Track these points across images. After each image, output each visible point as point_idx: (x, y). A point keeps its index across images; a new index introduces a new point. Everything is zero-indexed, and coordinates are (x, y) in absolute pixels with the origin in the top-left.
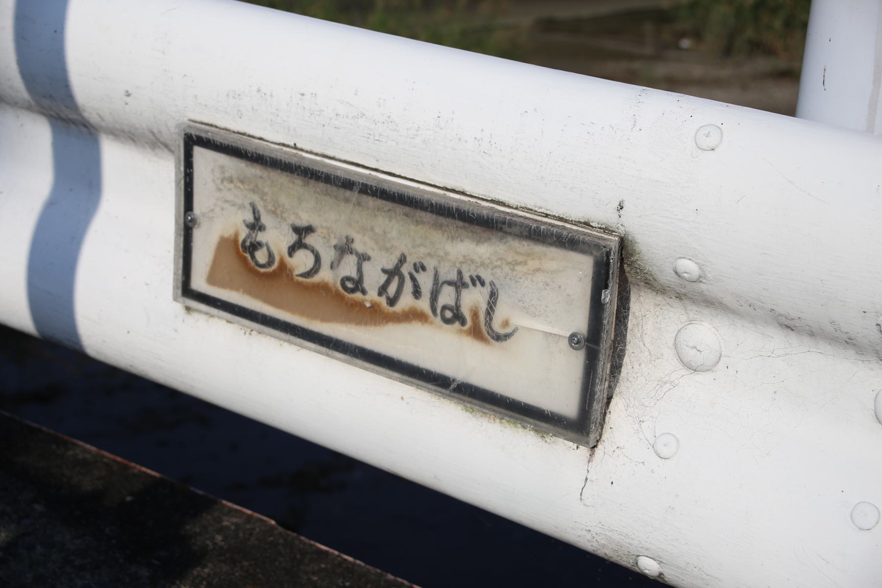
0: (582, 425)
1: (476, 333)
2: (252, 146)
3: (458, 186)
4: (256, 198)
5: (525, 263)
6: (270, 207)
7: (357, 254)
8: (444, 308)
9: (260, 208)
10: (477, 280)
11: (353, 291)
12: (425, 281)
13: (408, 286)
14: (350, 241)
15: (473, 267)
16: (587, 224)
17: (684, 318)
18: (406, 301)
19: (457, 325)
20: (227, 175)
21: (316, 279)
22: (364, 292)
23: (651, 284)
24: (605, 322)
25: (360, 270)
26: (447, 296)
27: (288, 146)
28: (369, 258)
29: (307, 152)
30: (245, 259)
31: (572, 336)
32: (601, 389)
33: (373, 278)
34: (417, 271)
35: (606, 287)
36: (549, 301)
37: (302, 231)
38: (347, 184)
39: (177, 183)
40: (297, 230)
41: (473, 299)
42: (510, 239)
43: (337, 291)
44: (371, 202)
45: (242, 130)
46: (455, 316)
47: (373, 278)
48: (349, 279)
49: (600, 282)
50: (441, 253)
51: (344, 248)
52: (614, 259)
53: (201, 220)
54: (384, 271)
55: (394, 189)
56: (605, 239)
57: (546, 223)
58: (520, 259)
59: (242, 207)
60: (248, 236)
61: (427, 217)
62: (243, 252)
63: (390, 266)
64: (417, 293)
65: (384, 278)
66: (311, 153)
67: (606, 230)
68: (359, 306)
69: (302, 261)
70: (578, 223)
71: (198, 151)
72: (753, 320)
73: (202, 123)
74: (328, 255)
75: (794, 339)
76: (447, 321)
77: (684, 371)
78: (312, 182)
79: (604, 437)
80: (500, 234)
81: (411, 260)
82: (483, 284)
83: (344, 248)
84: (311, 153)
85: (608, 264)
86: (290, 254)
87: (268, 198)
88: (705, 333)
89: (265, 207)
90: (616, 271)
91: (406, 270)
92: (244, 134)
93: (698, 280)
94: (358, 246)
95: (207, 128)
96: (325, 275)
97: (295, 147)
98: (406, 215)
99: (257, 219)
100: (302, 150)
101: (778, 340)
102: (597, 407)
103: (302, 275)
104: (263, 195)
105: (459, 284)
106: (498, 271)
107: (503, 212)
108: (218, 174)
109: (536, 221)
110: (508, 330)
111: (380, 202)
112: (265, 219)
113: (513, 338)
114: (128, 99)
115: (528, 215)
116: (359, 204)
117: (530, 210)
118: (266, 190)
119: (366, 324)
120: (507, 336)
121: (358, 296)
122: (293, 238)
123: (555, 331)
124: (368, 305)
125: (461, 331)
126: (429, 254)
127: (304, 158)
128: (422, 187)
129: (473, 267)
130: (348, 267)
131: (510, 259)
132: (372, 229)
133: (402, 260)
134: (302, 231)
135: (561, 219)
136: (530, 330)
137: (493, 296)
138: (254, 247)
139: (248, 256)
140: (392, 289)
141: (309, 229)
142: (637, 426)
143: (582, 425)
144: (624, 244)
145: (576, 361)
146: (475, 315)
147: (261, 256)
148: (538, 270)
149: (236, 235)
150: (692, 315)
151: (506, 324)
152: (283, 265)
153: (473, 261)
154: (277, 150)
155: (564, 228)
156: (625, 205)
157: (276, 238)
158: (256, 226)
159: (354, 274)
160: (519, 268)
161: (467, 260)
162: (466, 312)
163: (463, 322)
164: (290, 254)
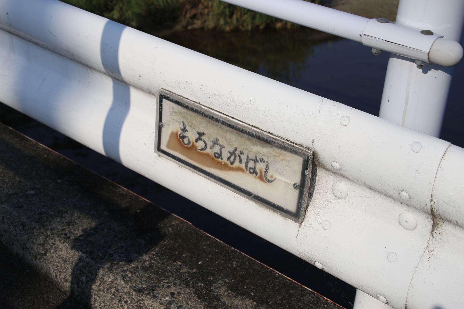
0: (297, 215)
1: (261, 178)
2: (184, 101)
3: (257, 126)
4: (184, 120)
5: (279, 157)
6: (189, 124)
7: (220, 145)
8: (250, 168)
9: (186, 123)
10: (262, 160)
11: (218, 158)
12: (244, 158)
13: (238, 159)
14: (217, 140)
15: (261, 155)
16: (301, 145)
17: (336, 180)
18: (237, 164)
19: (254, 174)
20: (175, 111)
21: (205, 152)
22: (222, 159)
23: (324, 167)
24: (306, 181)
25: (221, 151)
26: (251, 164)
27: (197, 103)
28: (224, 147)
29: (203, 106)
30: (180, 141)
31: (294, 185)
32: (304, 204)
33: (225, 154)
34: (241, 154)
35: (307, 169)
36: (287, 172)
37: (201, 134)
38: (217, 120)
39: (157, 111)
40: (199, 133)
41: (260, 166)
42: (274, 147)
43: (212, 157)
44: (225, 127)
45: (180, 94)
46: (254, 172)
47: (225, 154)
48: (217, 153)
49: (305, 167)
50: (250, 149)
51: (216, 142)
52: (310, 160)
53: (165, 125)
54: (229, 152)
55: (234, 124)
56: (307, 152)
57: (287, 144)
58: (277, 155)
59: (179, 122)
60: (181, 133)
61: (245, 136)
62: (179, 138)
63: (232, 151)
64: (241, 162)
65: (229, 155)
66: (205, 106)
67: (308, 148)
68: (220, 163)
69: (200, 145)
70: (298, 145)
71: (164, 101)
72: (359, 184)
73: (166, 90)
74: (209, 144)
75: (373, 192)
76: (251, 173)
77: (334, 198)
78: (205, 118)
79: (305, 220)
80: (271, 145)
81: (239, 150)
82: (264, 162)
83: (216, 142)
84: (205, 106)
85: (308, 161)
86: (196, 142)
87: (189, 121)
88: (343, 186)
89: (188, 124)
90: (311, 163)
91: (237, 153)
92: (181, 96)
93: (340, 169)
94: (220, 142)
95: (168, 92)
96: (208, 151)
97: (199, 103)
98: (238, 134)
99: (185, 128)
100: (202, 105)
101: (367, 192)
102: (302, 210)
103: (200, 150)
104: (187, 119)
105: (256, 161)
106: (269, 158)
107: (272, 138)
108: (171, 110)
109: (284, 142)
110: (273, 179)
111: (228, 128)
112: (187, 128)
113: (274, 182)
114: (140, 78)
115: (281, 140)
116: (221, 128)
117: (282, 138)
118: (188, 118)
119: (222, 170)
120: (272, 181)
121: (220, 159)
122: (198, 136)
123: (289, 182)
124: (223, 164)
125: (256, 177)
126: (245, 149)
127: (202, 108)
128: (244, 124)
129: (261, 155)
130: (217, 149)
131: (274, 154)
132: (225, 137)
133: (236, 149)
134: (201, 134)
135: (292, 142)
136: (279, 180)
137: (268, 166)
138: (184, 137)
139: (181, 140)
140: (232, 159)
141: (203, 134)
142: (316, 217)
143: (297, 215)
144: (314, 154)
145: (296, 193)
146: (261, 172)
147: (186, 141)
148: (284, 159)
149: (177, 132)
150: (338, 179)
151: (272, 177)
152: (193, 145)
153: (261, 153)
154: (192, 105)
155: (293, 146)
156: (315, 141)
157: (191, 135)
158: (184, 130)
159: (219, 152)
160: (277, 158)
161: (258, 152)
162: (258, 170)
163: (257, 174)
164: (196, 142)
